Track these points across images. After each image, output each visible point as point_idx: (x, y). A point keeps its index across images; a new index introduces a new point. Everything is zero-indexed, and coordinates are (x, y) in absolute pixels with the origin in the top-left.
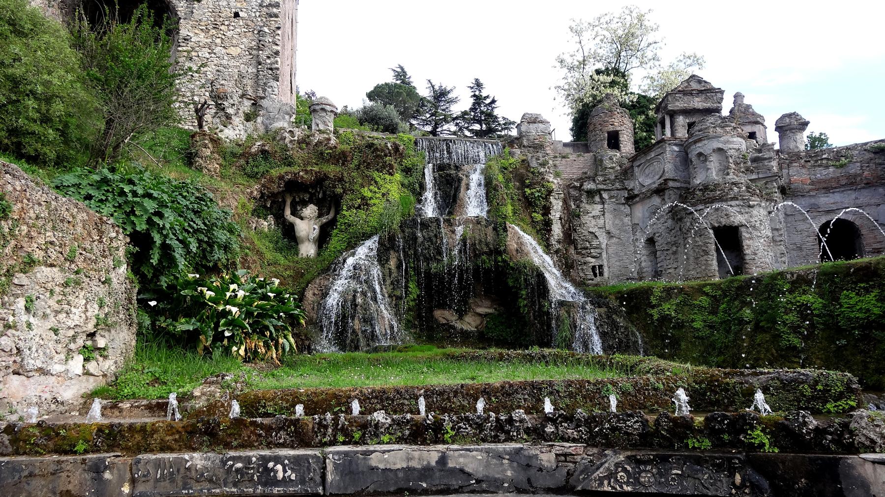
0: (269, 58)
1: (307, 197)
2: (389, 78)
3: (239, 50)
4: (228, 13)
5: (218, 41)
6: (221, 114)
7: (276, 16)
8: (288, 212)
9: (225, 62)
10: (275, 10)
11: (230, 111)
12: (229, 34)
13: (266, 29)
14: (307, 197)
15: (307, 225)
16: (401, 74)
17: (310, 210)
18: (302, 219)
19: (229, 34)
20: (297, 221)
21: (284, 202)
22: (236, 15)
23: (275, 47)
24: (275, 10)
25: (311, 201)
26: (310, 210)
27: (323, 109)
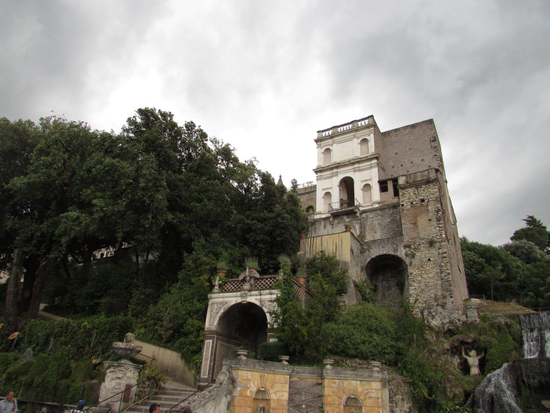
0: (446, 276)
1: (470, 347)
2: (524, 225)
3: (433, 275)
4: (426, 260)
5: (423, 272)
6: (430, 315)
7: (445, 257)
8: (463, 354)
9: (428, 281)
10: (445, 255)
11: (434, 314)
12: (427, 268)
13: (442, 264)
14: (470, 347)
15: (473, 360)
16: (532, 221)
17: (473, 353)
18: (470, 357)
19: (427, 268)
20: (468, 358)
21: (461, 348)
22: (429, 260)
23: (447, 271)
24: (445, 255)
25: (473, 348)
26: (473, 353)
27: (471, 308)
